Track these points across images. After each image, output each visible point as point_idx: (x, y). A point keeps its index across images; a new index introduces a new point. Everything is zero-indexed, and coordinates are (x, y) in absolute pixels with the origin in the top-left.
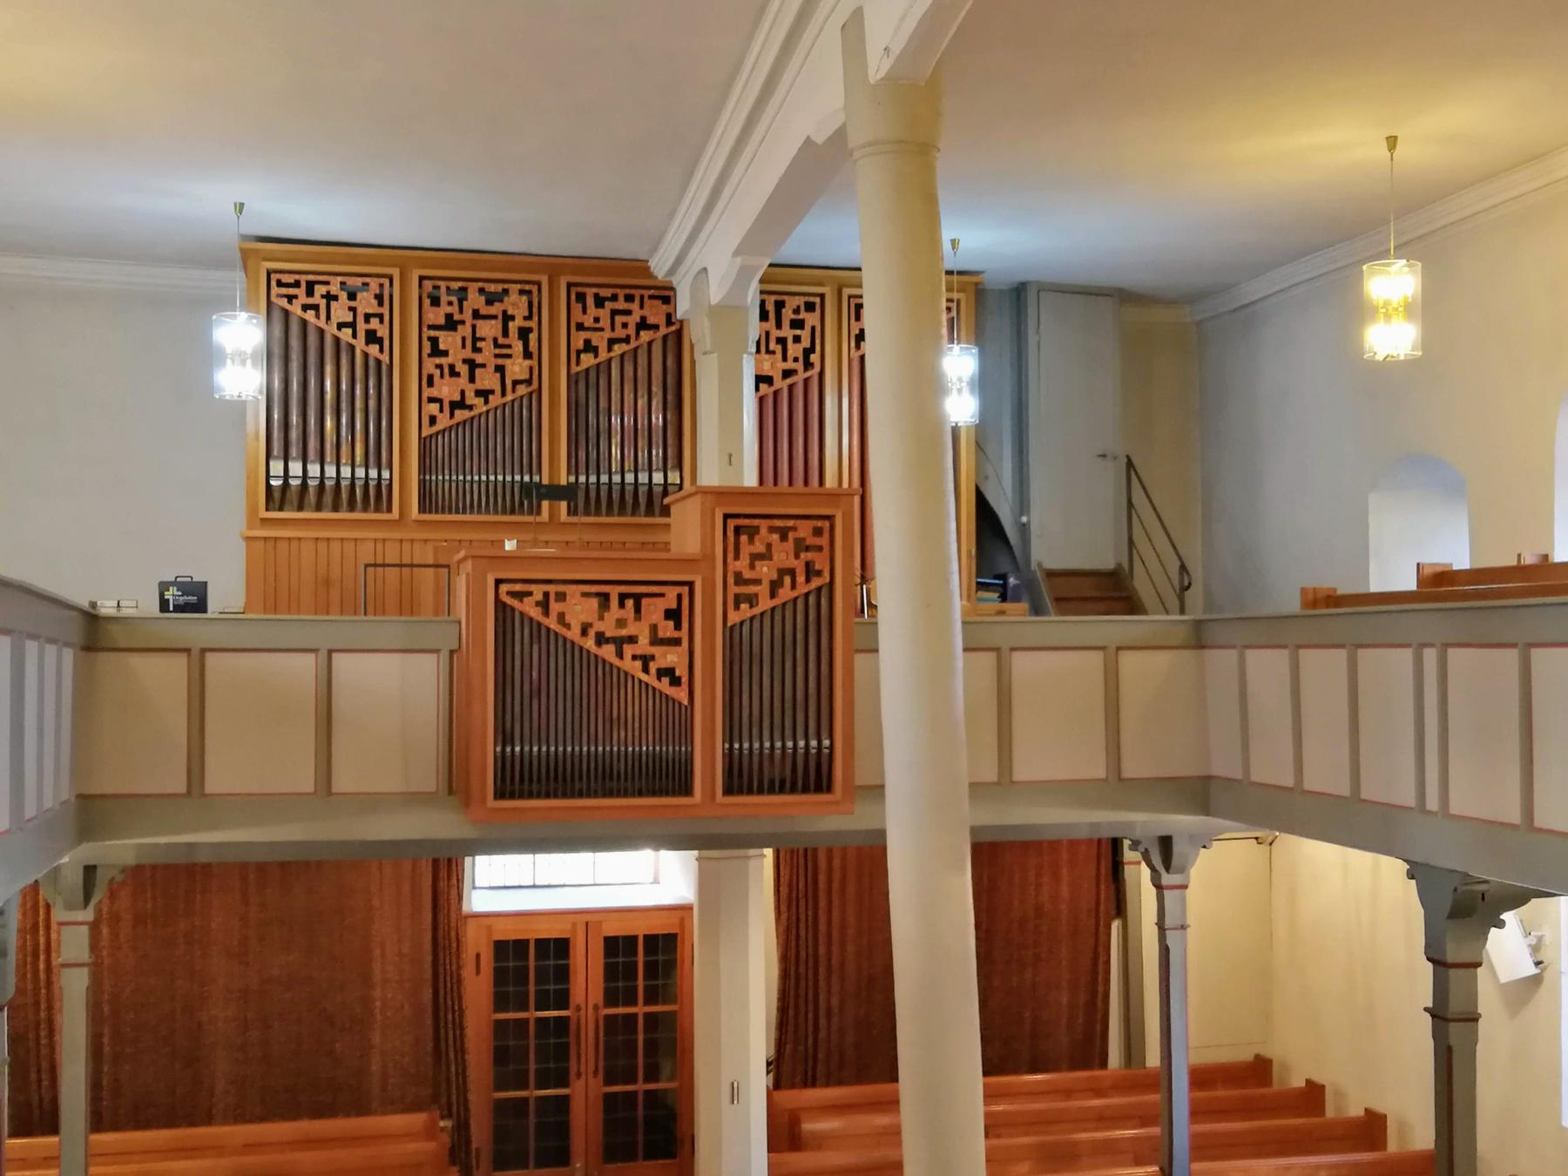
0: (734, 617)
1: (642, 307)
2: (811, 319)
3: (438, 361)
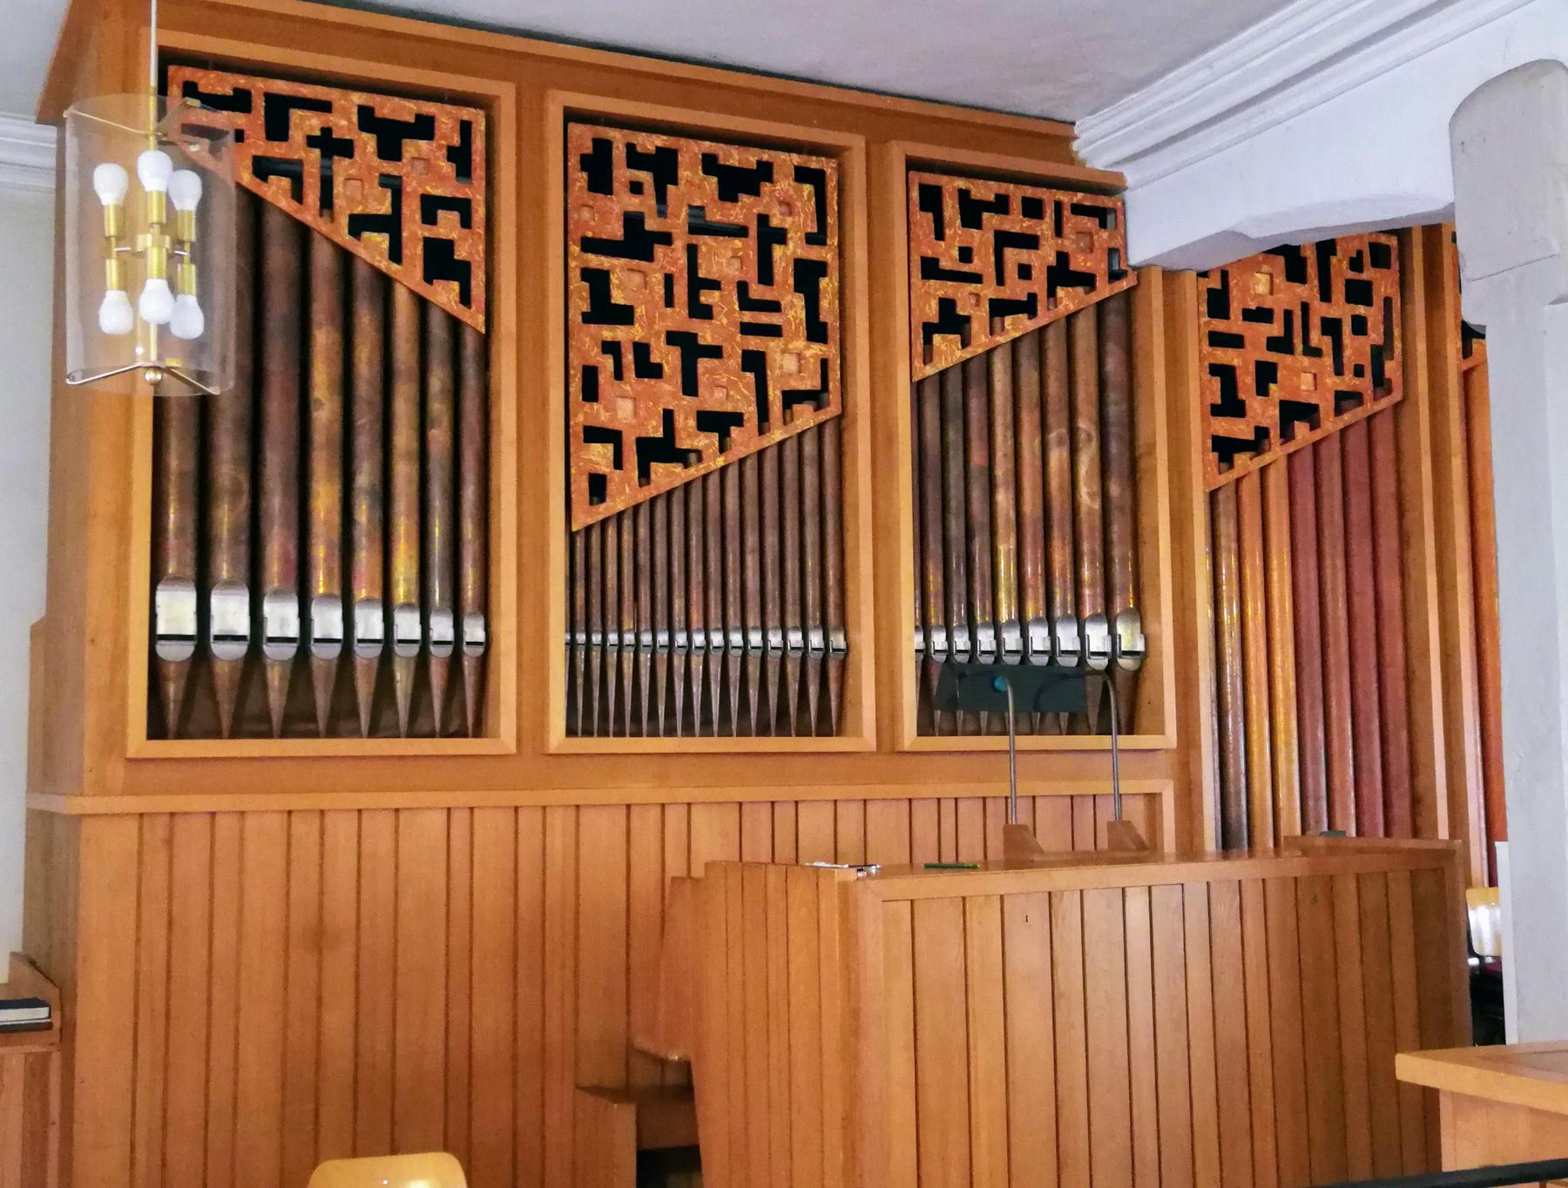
1: (1059, 232)
2: (1384, 283)
3: (608, 333)
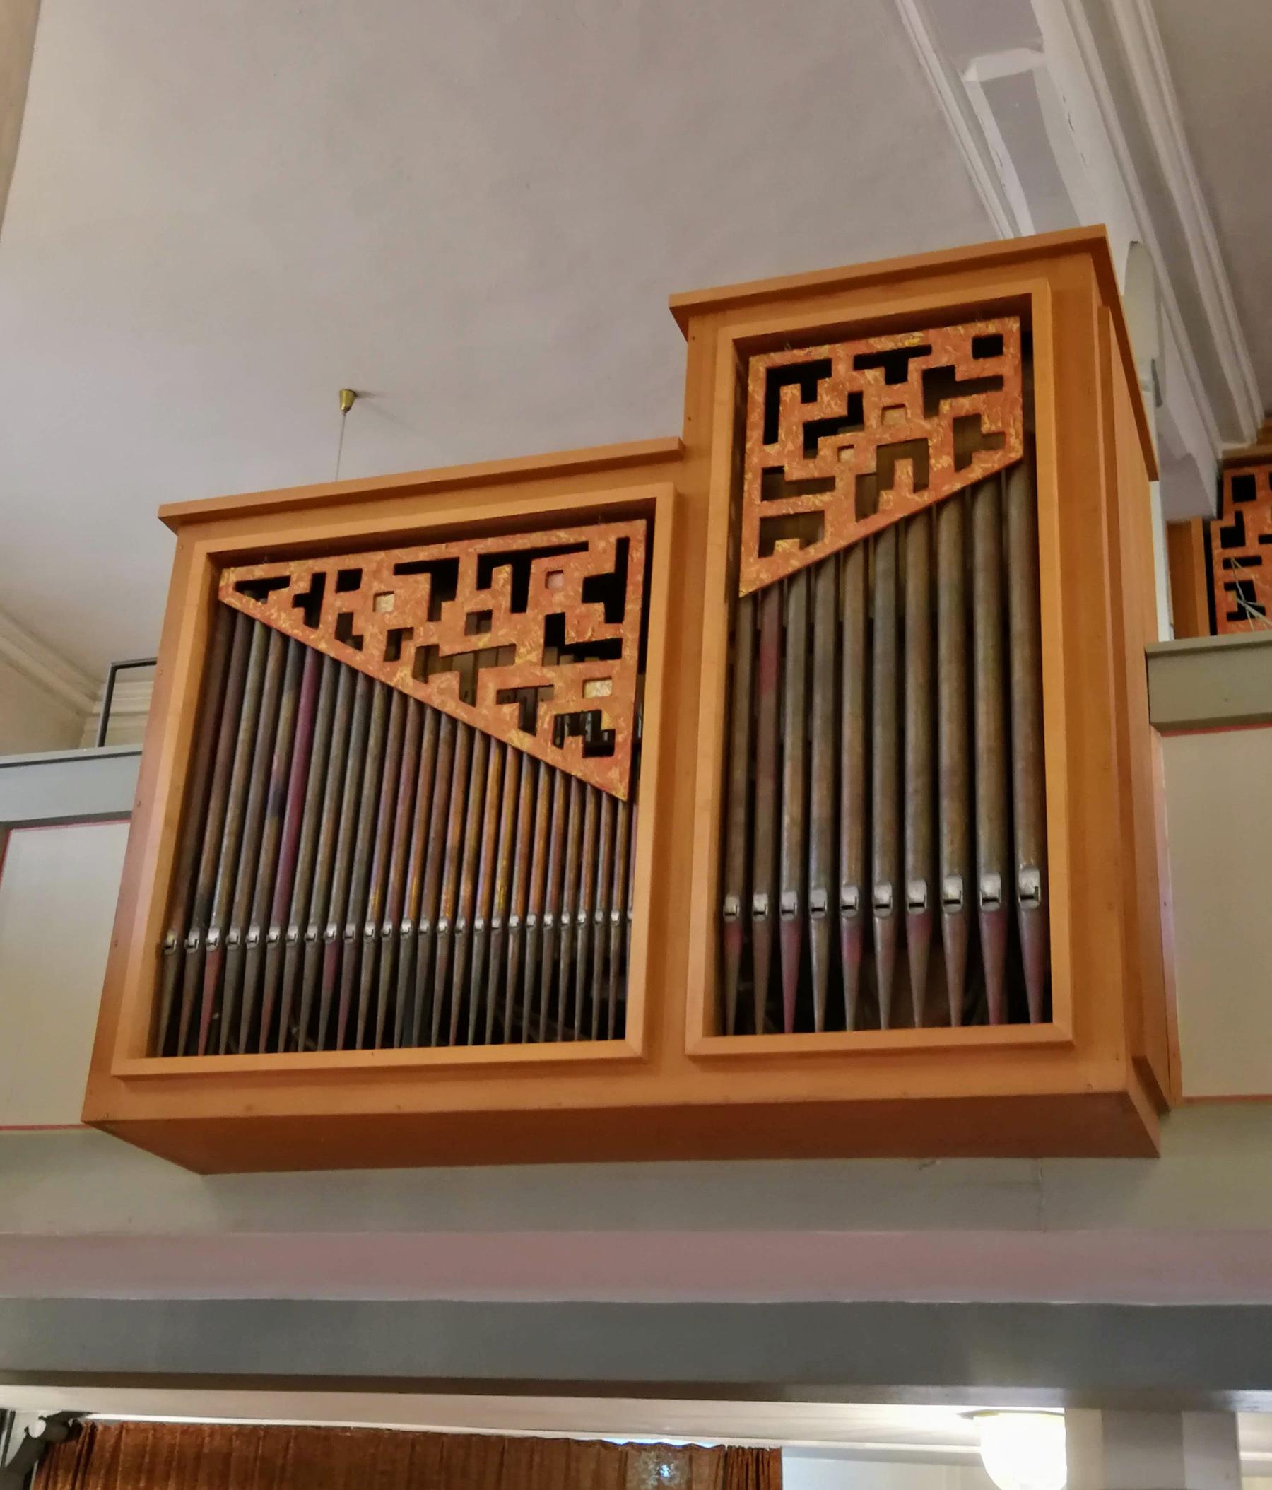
0: (756, 573)
